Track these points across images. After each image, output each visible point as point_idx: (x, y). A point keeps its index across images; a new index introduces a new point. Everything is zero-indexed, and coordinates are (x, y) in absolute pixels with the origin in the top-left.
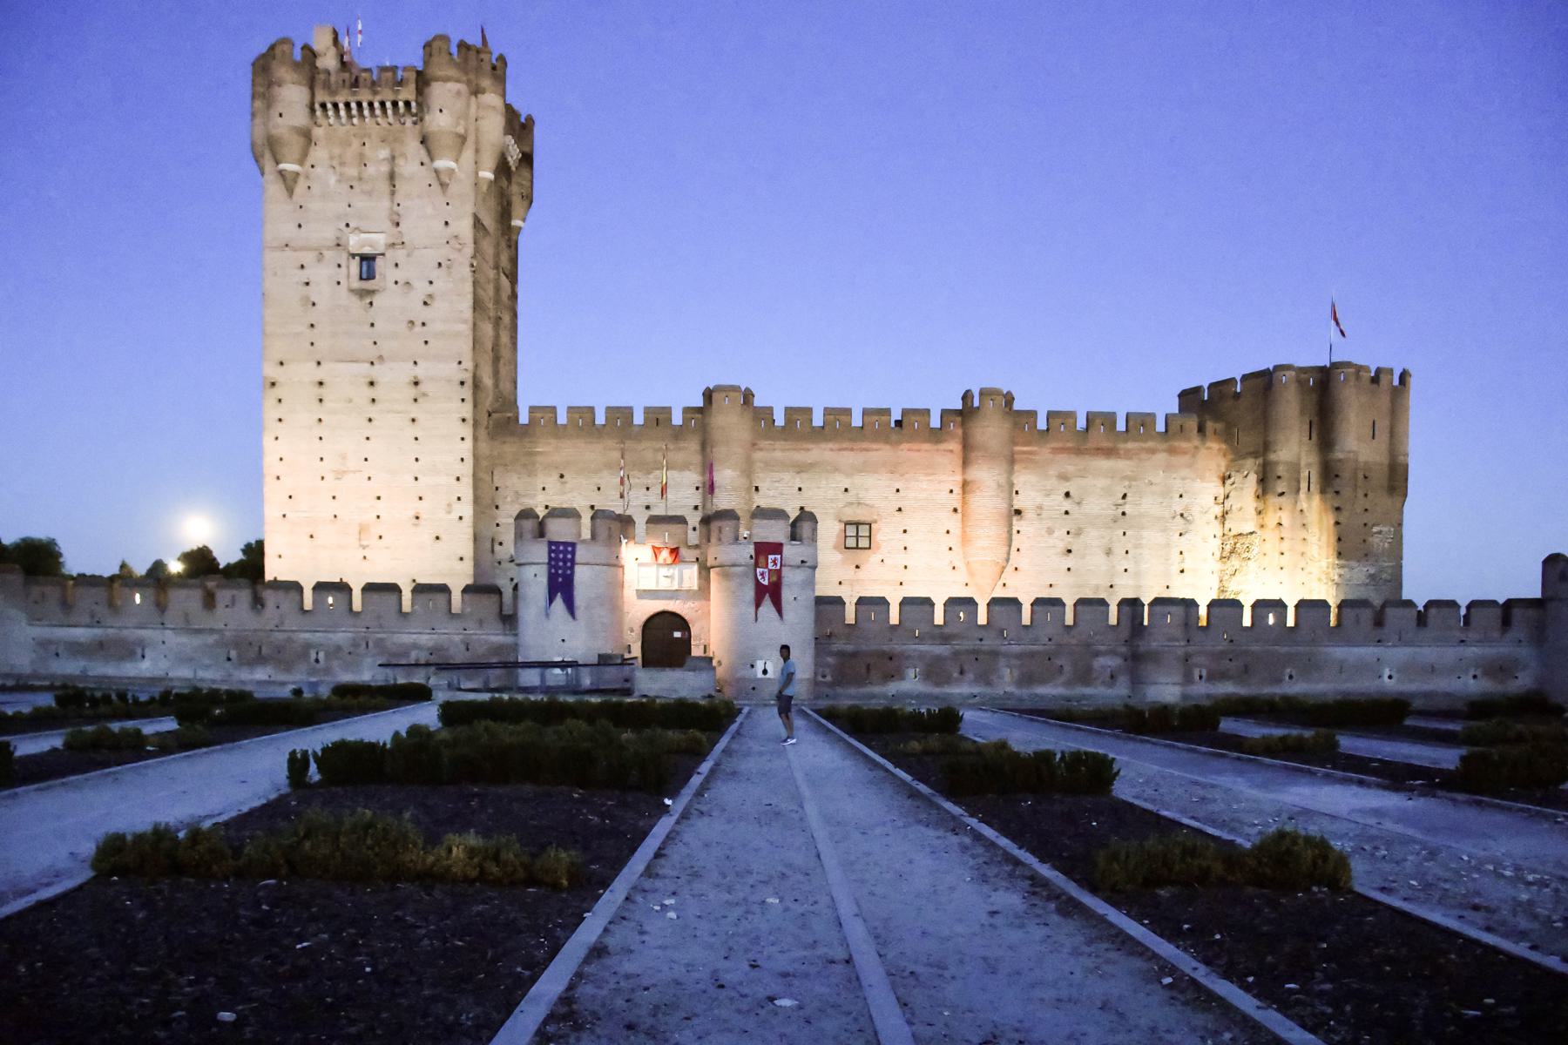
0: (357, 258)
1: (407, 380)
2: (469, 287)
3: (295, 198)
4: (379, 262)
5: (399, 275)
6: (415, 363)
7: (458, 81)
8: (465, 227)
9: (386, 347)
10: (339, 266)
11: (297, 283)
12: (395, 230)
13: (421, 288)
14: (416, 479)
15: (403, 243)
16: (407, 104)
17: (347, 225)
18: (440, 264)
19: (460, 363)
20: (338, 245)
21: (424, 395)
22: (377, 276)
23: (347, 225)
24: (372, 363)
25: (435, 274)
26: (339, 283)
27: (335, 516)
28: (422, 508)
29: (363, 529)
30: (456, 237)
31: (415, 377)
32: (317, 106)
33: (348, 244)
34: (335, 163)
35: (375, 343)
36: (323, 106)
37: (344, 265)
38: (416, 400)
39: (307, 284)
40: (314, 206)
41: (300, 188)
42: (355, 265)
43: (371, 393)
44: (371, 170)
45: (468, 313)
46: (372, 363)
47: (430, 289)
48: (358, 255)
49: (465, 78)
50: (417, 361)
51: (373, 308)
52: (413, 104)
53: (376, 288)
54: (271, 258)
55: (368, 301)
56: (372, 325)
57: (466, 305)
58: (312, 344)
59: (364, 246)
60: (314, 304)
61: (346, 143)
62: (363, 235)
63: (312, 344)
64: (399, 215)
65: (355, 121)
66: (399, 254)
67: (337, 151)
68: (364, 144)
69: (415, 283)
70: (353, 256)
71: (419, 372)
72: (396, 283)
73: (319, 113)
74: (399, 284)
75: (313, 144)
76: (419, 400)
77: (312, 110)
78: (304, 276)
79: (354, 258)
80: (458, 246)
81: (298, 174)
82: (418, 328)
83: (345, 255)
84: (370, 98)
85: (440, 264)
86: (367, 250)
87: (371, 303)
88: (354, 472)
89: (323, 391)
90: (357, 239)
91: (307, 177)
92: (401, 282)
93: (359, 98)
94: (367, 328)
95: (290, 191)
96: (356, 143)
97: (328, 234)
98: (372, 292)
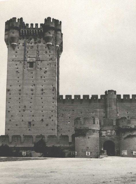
1: (40, 90)
11: (15, 68)
14: (42, 111)
21: (44, 93)
27: (23, 120)
28: (44, 118)
29: (30, 123)
31: (42, 89)
38: (42, 94)
41: (16, 48)
43: (31, 92)
62: (30, 58)
71: (43, 87)
76: (43, 94)
82: (43, 78)
83: (26, 62)
88: (28, 110)
89: (21, 92)
91: (18, 46)
94: (31, 78)
95: (14, 49)
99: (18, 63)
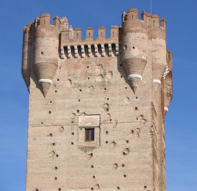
0: (84, 129)
2: (150, 143)
3: (47, 98)
4: (97, 131)
5: (108, 138)
6: (118, 188)
7: (142, 32)
8: (146, 111)
9: (100, 179)
10: (73, 134)
12: (106, 113)
13: (122, 145)
15: (111, 120)
16: (113, 45)
17: (78, 111)
18: (133, 131)
19: (145, 187)
20: (73, 122)
22: (95, 139)
23: (78, 111)
24: (92, 189)
25: (130, 136)
26: (72, 143)
30: (142, 116)
32: (62, 48)
33: (78, 122)
34: (70, 78)
35: (94, 177)
36: (66, 48)
37: (75, 133)
39: (54, 144)
40: (59, 101)
41: (50, 92)
42: (82, 134)
44: (92, 80)
45: (150, 159)
46: (92, 189)
47: (128, 145)
48: (84, 127)
49: (145, 30)
50: (120, 186)
51: (92, 157)
52: (117, 45)
53: (95, 146)
54: (31, 131)
55: (90, 153)
56: (92, 167)
57: (148, 153)
58: (56, 178)
59: (88, 123)
60: (57, 156)
61: (76, 67)
62: (87, 117)
63: (56, 178)
64: (108, 105)
65: (84, 55)
66: (109, 127)
67: (72, 72)
68: (88, 67)
69: (118, 142)
70: (81, 128)
72: (107, 142)
73: (63, 52)
74: (109, 143)
75: (59, 68)
77: (60, 50)
78: (51, 140)
79: (81, 129)
80: (143, 121)
81: (50, 84)
82: (120, 168)
83: (76, 128)
84: (92, 43)
85: (133, 131)
86: (89, 125)
87: (92, 154)
90: (84, 118)
92: (110, 142)
93: (85, 43)
96: (83, 67)
97: (68, 116)
98: (93, 148)
99: (55, 129)
